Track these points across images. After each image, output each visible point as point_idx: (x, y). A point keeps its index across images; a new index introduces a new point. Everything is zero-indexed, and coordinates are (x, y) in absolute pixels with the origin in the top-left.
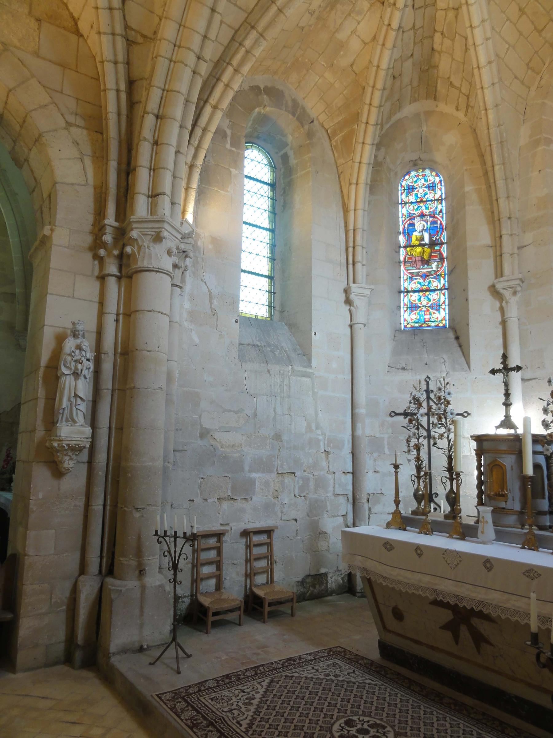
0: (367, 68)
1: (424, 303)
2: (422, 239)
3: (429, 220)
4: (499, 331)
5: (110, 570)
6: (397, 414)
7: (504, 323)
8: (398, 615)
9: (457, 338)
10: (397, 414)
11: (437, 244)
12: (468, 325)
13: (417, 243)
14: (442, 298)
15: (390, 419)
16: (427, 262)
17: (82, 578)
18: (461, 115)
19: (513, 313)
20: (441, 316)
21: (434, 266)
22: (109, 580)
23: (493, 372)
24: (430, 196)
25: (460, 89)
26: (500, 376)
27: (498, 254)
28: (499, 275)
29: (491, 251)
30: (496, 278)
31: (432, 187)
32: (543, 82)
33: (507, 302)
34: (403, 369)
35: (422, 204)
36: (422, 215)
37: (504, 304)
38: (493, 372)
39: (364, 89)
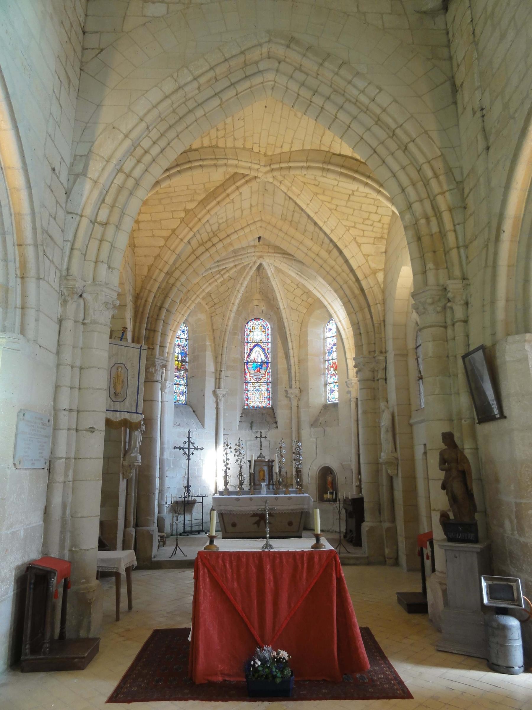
0: (195, 285)
1: (178, 391)
2: (178, 357)
3: (182, 348)
4: (215, 411)
5: (137, 525)
6: (177, 448)
7: (217, 409)
8: (234, 525)
9: (194, 412)
10: (177, 448)
11: (184, 362)
12: (204, 407)
13: (176, 359)
14: (183, 388)
15: (174, 450)
16: (179, 370)
17: (127, 529)
18: (207, 307)
19: (222, 405)
20: (183, 398)
21: (182, 372)
22: (138, 528)
23: (256, 437)
24: (182, 336)
25: (213, 300)
26: (259, 439)
27: (218, 377)
28: (217, 387)
29: (214, 375)
30: (216, 388)
31: (183, 331)
32: (240, 309)
33: (220, 400)
34: (179, 425)
35: (179, 339)
36: (178, 345)
37: (218, 400)
38: (256, 437)
39: (189, 291)
